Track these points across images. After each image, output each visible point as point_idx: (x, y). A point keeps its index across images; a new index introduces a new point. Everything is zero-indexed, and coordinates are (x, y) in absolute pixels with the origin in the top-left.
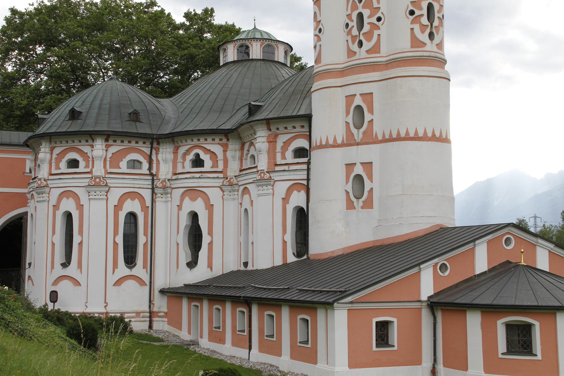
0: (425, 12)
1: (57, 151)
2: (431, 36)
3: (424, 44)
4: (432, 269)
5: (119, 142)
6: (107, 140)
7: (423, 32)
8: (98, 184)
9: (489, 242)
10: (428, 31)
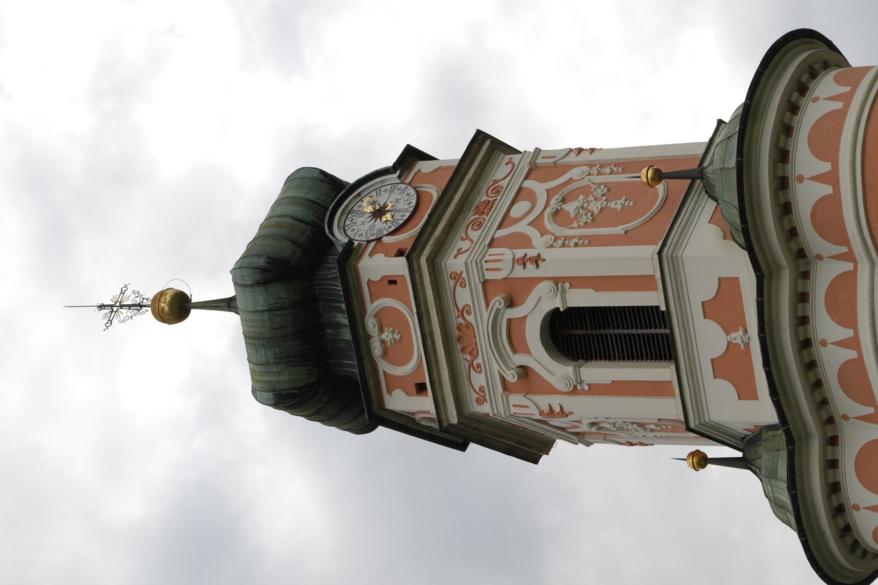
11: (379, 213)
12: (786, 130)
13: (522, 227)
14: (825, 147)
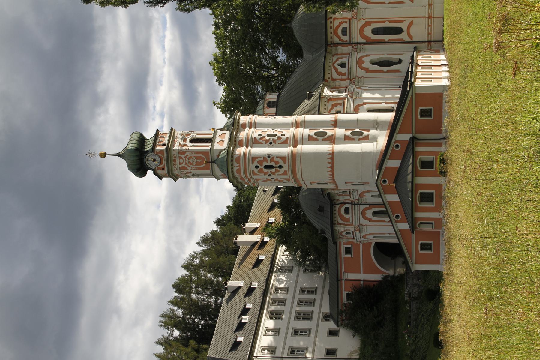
0: (269, 170)
1: (340, 221)
2: (281, 167)
3: (285, 171)
4: (398, 224)
5: (336, 219)
6: (335, 224)
7: (279, 171)
8: (359, 228)
9: (385, 194)
10: (278, 169)
11: (154, 160)
12: (232, 171)
13: (183, 165)
14: (239, 171)
